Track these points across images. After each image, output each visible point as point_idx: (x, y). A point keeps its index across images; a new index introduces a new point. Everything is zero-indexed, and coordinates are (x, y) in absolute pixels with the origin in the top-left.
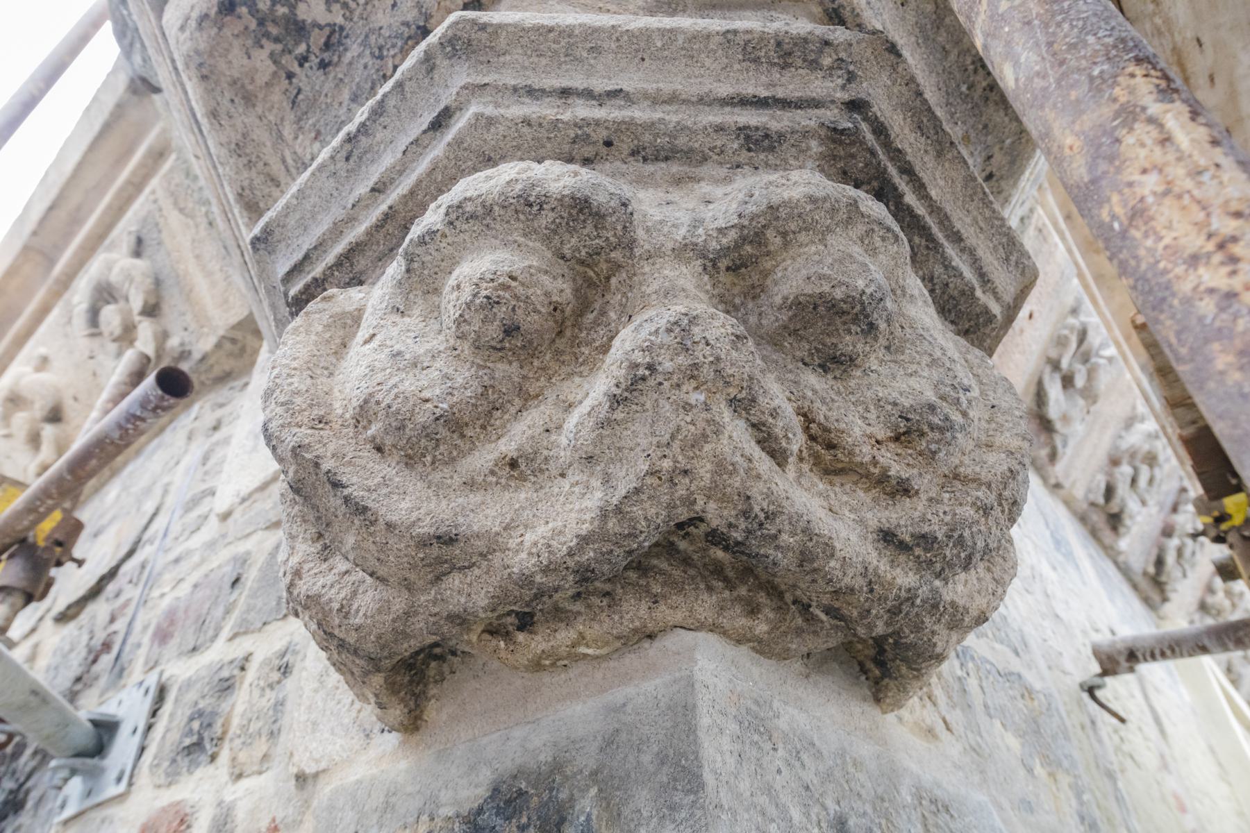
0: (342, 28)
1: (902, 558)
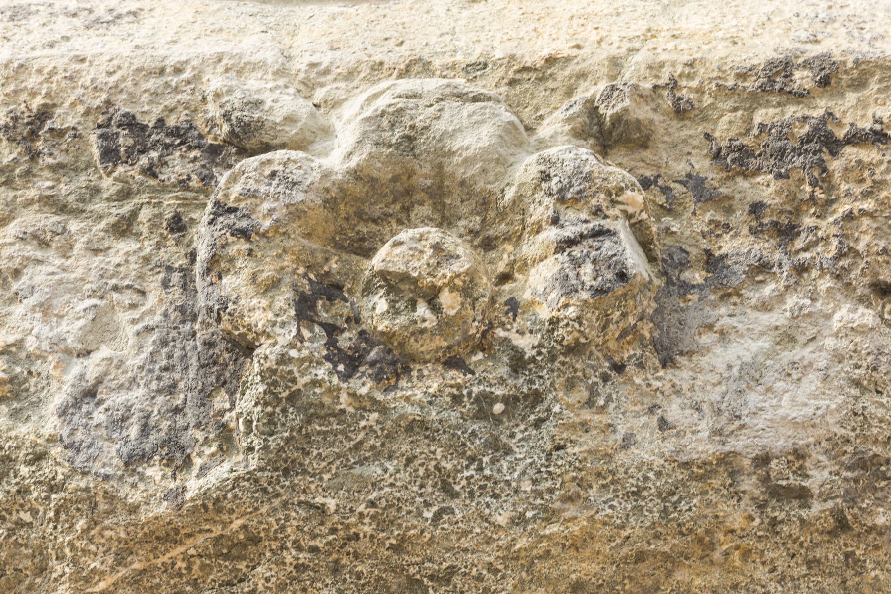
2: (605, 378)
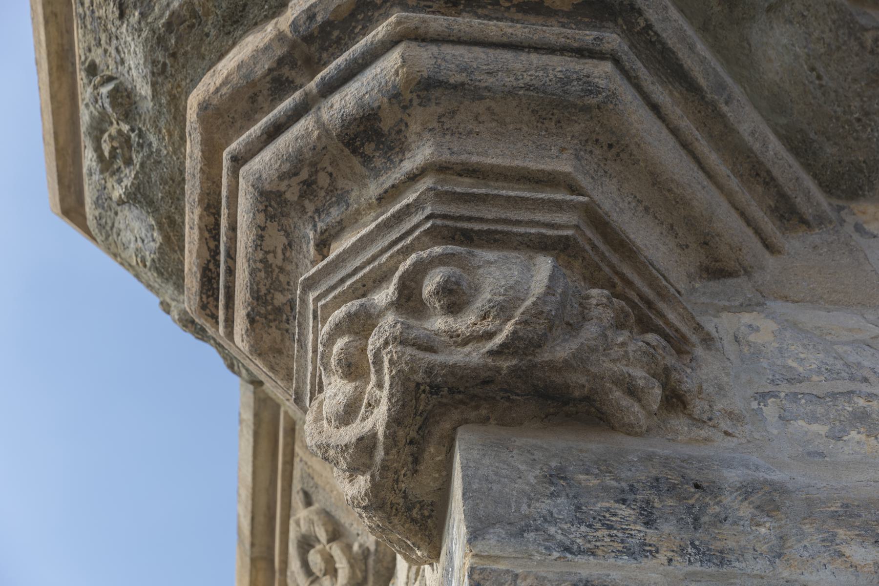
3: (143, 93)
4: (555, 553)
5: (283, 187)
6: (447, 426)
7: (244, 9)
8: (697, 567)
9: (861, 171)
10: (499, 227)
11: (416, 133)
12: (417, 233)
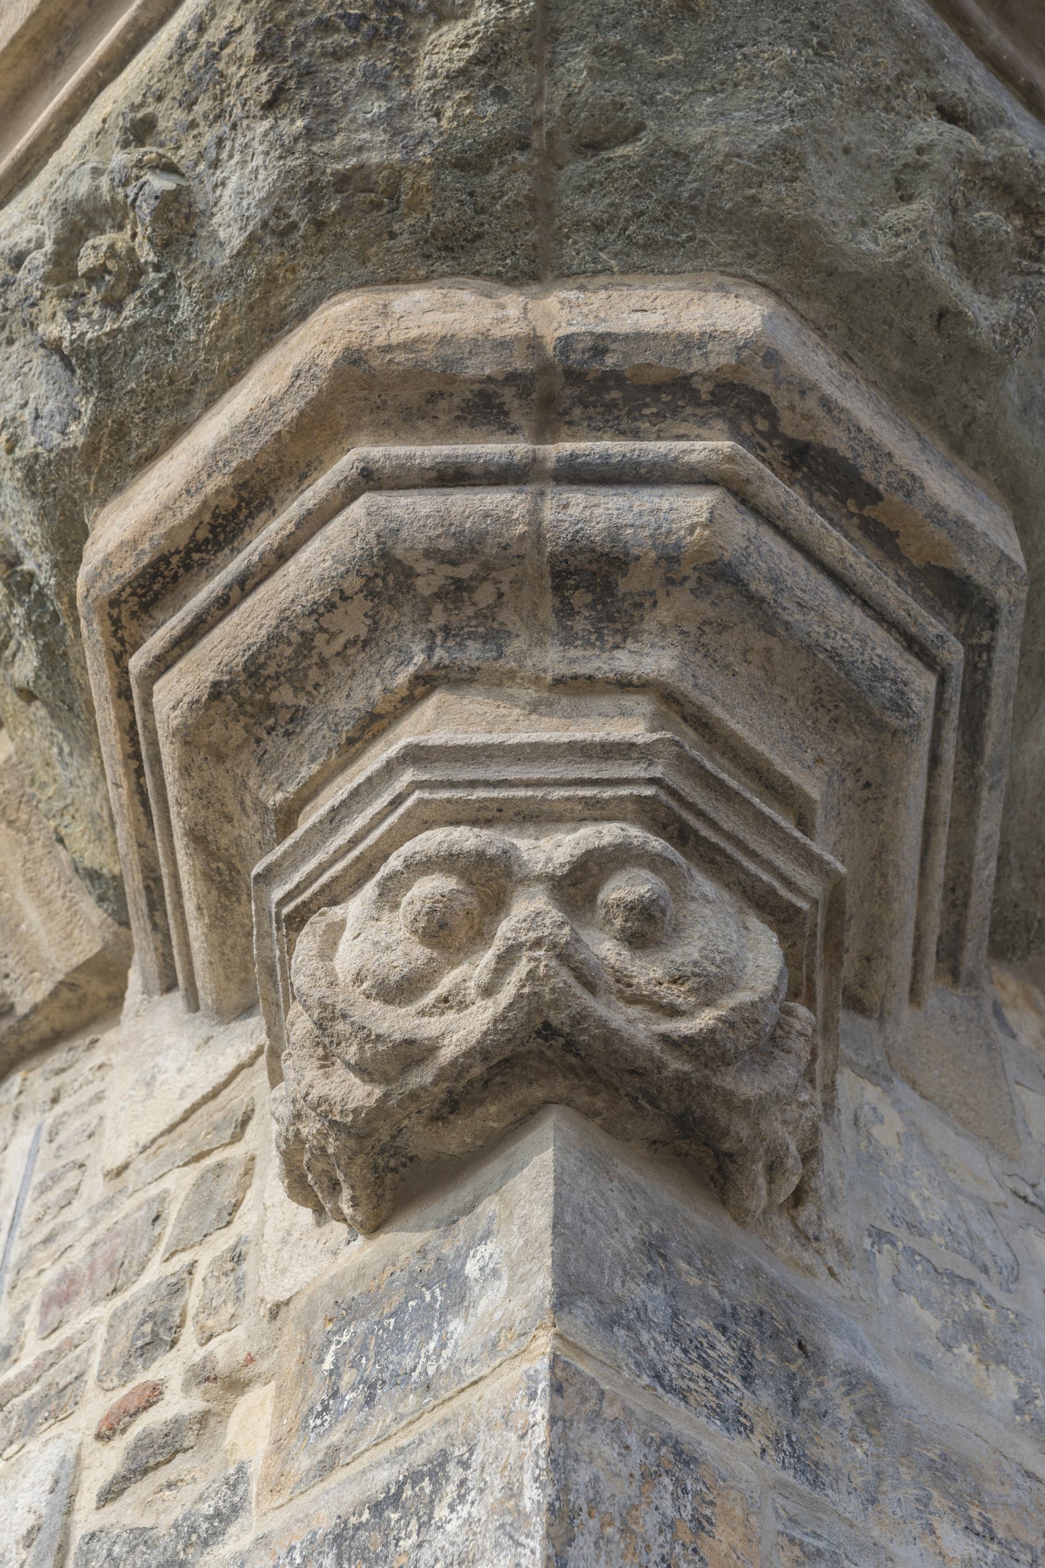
0: (305, 709)
1: (677, 1053)
2: (190, 244)
3: (222, 234)
4: (644, 1377)
5: (421, 567)
6: (539, 1093)
7: (473, 240)
8: (788, 1476)
9: (1028, 930)
10: (729, 848)
11: (660, 623)
12: (624, 791)
